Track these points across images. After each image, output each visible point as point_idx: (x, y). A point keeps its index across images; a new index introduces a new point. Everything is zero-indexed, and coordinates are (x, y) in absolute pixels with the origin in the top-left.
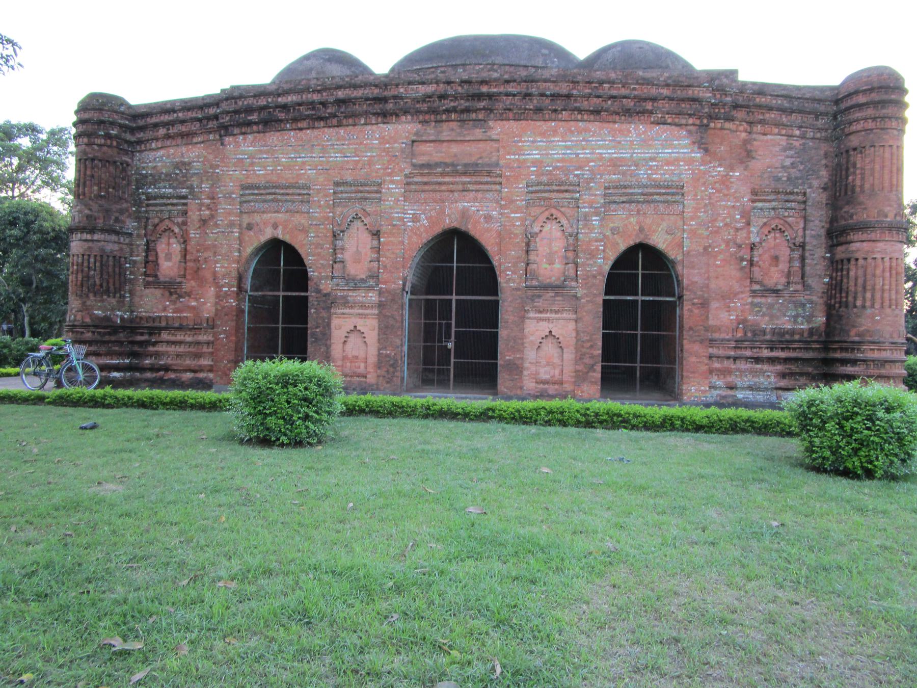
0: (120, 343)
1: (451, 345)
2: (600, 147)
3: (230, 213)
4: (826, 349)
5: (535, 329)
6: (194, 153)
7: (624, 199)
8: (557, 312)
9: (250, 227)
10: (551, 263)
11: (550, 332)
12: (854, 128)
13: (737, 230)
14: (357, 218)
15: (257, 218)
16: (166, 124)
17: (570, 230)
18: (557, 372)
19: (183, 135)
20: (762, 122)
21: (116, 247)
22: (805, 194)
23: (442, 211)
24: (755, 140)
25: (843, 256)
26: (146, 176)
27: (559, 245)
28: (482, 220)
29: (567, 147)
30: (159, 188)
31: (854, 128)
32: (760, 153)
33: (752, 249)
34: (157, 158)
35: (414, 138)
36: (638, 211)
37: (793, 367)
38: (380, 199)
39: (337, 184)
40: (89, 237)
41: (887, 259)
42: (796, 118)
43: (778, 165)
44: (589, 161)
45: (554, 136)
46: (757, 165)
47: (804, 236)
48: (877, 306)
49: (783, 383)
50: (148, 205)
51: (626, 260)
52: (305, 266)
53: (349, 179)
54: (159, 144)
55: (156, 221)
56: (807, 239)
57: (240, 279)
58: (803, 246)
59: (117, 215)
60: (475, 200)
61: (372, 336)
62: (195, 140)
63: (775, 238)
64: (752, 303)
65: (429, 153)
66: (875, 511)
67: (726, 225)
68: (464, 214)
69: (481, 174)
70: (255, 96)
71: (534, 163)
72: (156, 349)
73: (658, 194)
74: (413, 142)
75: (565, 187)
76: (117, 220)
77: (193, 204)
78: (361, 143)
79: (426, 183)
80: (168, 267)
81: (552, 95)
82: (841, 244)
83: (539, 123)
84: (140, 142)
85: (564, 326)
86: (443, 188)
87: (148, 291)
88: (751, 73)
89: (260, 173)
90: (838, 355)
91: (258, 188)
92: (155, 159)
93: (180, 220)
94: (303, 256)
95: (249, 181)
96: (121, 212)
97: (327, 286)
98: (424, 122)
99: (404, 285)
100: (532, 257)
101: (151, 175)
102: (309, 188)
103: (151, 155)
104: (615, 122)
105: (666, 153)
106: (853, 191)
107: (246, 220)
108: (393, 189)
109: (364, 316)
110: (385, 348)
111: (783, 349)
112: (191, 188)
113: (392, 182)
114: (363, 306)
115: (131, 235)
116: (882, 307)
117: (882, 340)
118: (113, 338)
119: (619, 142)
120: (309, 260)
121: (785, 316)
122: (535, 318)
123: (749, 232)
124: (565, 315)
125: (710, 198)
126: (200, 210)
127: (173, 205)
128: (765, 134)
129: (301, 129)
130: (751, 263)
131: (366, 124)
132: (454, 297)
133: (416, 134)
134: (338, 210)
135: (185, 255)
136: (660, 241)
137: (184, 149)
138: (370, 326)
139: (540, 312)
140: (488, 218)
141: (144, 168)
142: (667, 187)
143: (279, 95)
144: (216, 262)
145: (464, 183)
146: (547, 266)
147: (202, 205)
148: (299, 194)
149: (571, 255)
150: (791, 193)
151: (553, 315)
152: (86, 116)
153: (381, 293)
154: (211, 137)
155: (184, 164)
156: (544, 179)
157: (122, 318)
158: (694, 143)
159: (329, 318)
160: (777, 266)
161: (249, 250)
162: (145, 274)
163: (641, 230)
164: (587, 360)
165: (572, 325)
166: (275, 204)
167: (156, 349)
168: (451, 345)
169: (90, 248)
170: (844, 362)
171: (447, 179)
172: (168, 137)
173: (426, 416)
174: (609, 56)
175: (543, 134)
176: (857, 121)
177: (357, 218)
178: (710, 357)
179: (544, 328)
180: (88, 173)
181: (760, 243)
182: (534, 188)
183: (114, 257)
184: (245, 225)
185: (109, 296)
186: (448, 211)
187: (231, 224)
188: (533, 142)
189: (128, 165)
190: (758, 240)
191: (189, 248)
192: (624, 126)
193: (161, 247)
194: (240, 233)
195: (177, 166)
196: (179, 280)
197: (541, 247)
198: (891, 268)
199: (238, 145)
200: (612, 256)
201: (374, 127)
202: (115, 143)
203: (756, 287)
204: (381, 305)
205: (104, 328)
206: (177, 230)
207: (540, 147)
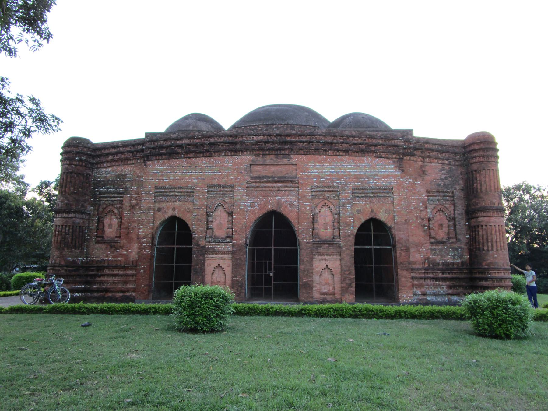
0: (80, 276)
1: (271, 274)
2: (349, 169)
3: (148, 202)
4: (471, 273)
5: (319, 264)
6: (128, 170)
7: (362, 195)
8: (330, 255)
9: (159, 210)
10: (326, 229)
11: (327, 266)
12: (474, 161)
13: (421, 211)
14: (220, 205)
15: (164, 205)
16: (113, 154)
17: (335, 211)
18: (331, 288)
19: (122, 160)
20: (429, 157)
21: (81, 221)
22: (453, 193)
23: (267, 202)
24: (426, 165)
25: (475, 224)
26: (100, 182)
27: (329, 219)
28: (288, 206)
29: (332, 169)
30: (107, 188)
31: (474, 161)
32: (429, 172)
33: (429, 220)
34: (107, 172)
35: (252, 163)
36: (370, 201)
37: (455, 283)
38: (233, 195)
39: (209, 187)
40: (66, 215)
41: (497, 226)
42: (446, 155)
43: (438, 178)
44: (343, 176)
45: (325, 163)
46: (428, 178)
47: (454, 214)
48: (495, 250)
49: (450, 291)
50: (100, 198)
51: (365, 227)
52: (190, 230)
53: (216, 184)
54: (109, 165)
55: (104, 206)
56: (456, 216)
57: (153, 238)
58: (454, 219)
59: (83, 203)
60: (284, 195)
62: (129, 163)
63: (440, 215)
64: (431, 249)
65: (259, 171)
66: (516, 353)
67: (415, 208)
68: (279, 203)
69: (287, 182)
70: (164, 140)
71: (316, 176)
72: (100, 279)
73: (380, 193)
74: (251, 165)
75: (332, 189)
76: (83, 206)
77: (126, 197)
78: (223, 166)
79: (258, 187)
80: (110, 232)
81: (323, 143)
82: (473, 218)
83: (317, 156)
84: (97, 163)
85: (334, 263)
86: (267, 189)
87: (97, 245)
88: (421, 132)
89: (166, 181)
90: (478, 276)
91: (165, 189)
92: (106, 172)
93: (118, 206)
94: (190, 226)
95: (160, 185)
96: (85, 201)
97: (203, 242)
98: (256, 155)
99: (246, 240)
100: (316, 226)
101: (103, 181)
102: (194, 189)
103: (104, 170)
104: (356, 156)
105: (383, 172)
106: (477, 192)
107: (157, 206)
110: (236, 277)
111: (449, 273)
112: (126, 188)
113: (240, 186)
114: (223, 253)
115: (89, 214)
116: (497, 250)
117: (499, 267)
118: (77, 273)
119: (359, 166)
120: (193, 228)
121: (448, 255)
122: (318, 259)
123: (427, 212)
124: (334, 257)
125: (406, 195)
126: (131, 200)
127: (114, 197)
128: (431, 163)
129: (189, 158)
130: (429, 228)
131: (225, 156)
132: (273, 248)
133: (253, 161)
134: (210, 201)
135: (121, 225)
136: (382, 217)
137: (123, 167)
138: (227, 264)
139: (321, 255)
140: (292, 205)
141: (99, 177)
142: (384, 189)
143: (178, 140)
144: (140, 229)
145: (278, 187)
146: (324, 230)
147: (131, 197)
148: (188, 192)
149: (336, 224)
150: (446, 192)
151: (328, 257)
152: (69, 149)
153: (233, 245)
154: (139, 161)
155: (122, 175)
156: (321, 185)
157: (82, 261)
158: (396, 167)
159: (204, 260)
160: (442, 229)
161: (158, 222)
162: (97, 236)
163: (372, 211)
164: (348, 281)
165: (338, 262)
166: (174, 197)
167: (100, 279)
168: (271, 274)
169: (66, 221)
170: (481, 279)
171: (269, 185)
172: (113, 160)
173: (268, 315)
174: (347, 121)
175: (319, 162)
176: (475, 157)
177: (220, 205)
178: (412, 278)
179: (323, 264)
180: (69, 180)
181: (433, 217)
182: (315, 190)
183: (80, 227)
184: (156, 209)
185: (75, 249)
186: (270, 201)
187: (149, 208)
188: (314, 166)
189: (90, 175)
190: (431, 216)
191: (123, 221)
192: (361, 158)
193: (106, 221)
194: (154, 213)
195: (118, 176)
196: (116, 239)
197: (320, 220)
198: (499, 230)
199: (154, 165)
200: (358, 225)
201: (230, 157)
202: (84, 164)
203: (433, 240)
204: (233, 253)
205: (73, 267)
206: (116, 211)
207: (318, 169)
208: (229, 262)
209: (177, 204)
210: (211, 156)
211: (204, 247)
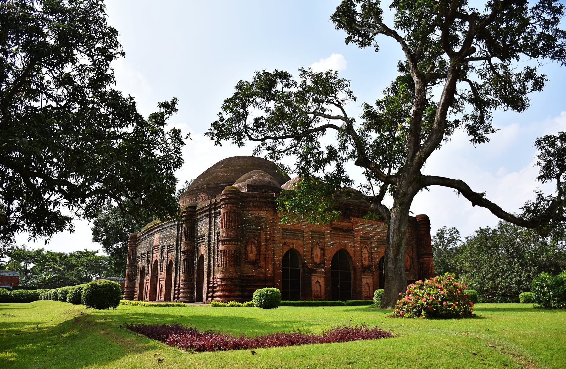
3: (280, 238)
10: (366, 261)
16: (253, 202)
19: (259, 207)
23: (339, 244)
61: (322, 283)
69: (349, 231)
71: (362, 231)
75: (368, 239)
77: (263, 233)
80: (252, 256)
108: (327, 234)
112: (262, 227)
114: (320, 273)
138: (322, 280)
153: (325, 269)
162: (245, 259)
165: (372, 280)
172: (254, 206)
187: (280, 242)
193: (249, 248)
195: (257, 218)
204: (325, 273)
208: (323, 279)
209: (294, 241)
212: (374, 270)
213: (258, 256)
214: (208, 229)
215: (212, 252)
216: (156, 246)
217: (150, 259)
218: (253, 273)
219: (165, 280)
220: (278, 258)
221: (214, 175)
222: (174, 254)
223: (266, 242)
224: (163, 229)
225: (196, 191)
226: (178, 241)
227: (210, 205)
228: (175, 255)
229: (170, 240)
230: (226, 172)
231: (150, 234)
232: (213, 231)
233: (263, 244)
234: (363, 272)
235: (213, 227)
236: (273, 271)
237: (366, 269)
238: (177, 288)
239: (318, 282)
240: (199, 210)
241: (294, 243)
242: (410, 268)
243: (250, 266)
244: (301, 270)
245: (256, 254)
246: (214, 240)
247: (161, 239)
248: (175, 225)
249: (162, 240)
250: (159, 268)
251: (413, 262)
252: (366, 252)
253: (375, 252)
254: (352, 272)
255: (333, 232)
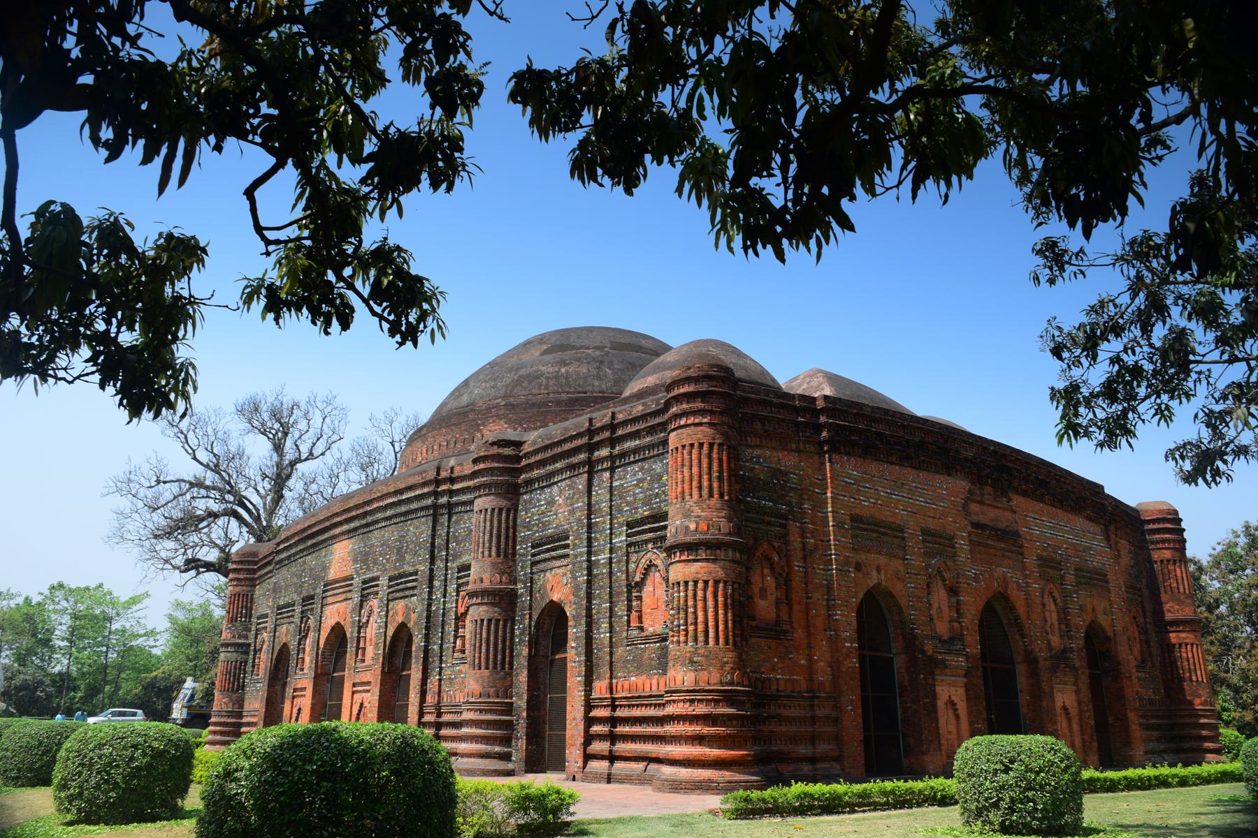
16: (764, 420)
77: (794, 527)
80: (765, 607)
90: (1187, 720)
98: (973, 484)
101: (749, 478)
108: (962, 544)
109: (953, 684)
112: (789, 504)
127: (769, 523)
129: (892, 463)
165: (1073, 697)
171: (990, 542)
193: (756, 579)
208: (961, 691)
209: (883, 560)
210: (919, 468)
211: (929, 657)
212: (1078, 664)
213: (784, 608)
214: (581, 514)
215: (601, 592)
216: (336, 581)
217: (312, 622)
218: (773, 670)
219: (376, 690)
220: (846, 618)
221: (523, 372)
222: (416, 603)
223: (804, 559)
224: (368, 525)
225: (471, 416)
226: (433, 560)
227: (591, 432)
228: (421, 608)
229: (401, 558)
230: (563, 363)
231: (314, 545)
232: (602, 521)
233: (797, 565)
234: (1054, 669)
235: (605, 506)
236: (835, 664)
237: (1060, 659)
238: (428, 718)
239: (951, 703)
240: (536, 452)
241: (882, 570)
242: (1143, 661)
243: (763, 643)
244: (899, 662)
245: (778, 603)
246: (611, 551)
247: (363, 558)
248: (427, 508)
249: (365, 561)
250: (351, 649)
251: (1147, 642)
252: (1053, 607)
253: (1074, 609)
254: (1021, 671)
255: (973, 537)
